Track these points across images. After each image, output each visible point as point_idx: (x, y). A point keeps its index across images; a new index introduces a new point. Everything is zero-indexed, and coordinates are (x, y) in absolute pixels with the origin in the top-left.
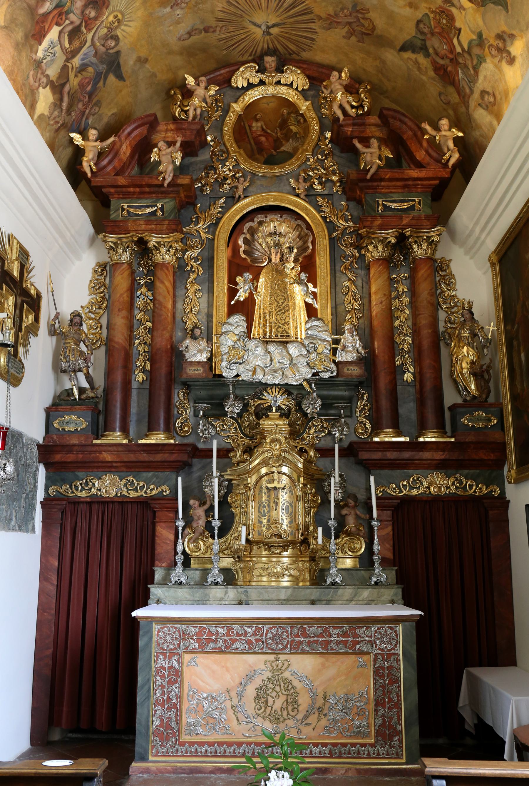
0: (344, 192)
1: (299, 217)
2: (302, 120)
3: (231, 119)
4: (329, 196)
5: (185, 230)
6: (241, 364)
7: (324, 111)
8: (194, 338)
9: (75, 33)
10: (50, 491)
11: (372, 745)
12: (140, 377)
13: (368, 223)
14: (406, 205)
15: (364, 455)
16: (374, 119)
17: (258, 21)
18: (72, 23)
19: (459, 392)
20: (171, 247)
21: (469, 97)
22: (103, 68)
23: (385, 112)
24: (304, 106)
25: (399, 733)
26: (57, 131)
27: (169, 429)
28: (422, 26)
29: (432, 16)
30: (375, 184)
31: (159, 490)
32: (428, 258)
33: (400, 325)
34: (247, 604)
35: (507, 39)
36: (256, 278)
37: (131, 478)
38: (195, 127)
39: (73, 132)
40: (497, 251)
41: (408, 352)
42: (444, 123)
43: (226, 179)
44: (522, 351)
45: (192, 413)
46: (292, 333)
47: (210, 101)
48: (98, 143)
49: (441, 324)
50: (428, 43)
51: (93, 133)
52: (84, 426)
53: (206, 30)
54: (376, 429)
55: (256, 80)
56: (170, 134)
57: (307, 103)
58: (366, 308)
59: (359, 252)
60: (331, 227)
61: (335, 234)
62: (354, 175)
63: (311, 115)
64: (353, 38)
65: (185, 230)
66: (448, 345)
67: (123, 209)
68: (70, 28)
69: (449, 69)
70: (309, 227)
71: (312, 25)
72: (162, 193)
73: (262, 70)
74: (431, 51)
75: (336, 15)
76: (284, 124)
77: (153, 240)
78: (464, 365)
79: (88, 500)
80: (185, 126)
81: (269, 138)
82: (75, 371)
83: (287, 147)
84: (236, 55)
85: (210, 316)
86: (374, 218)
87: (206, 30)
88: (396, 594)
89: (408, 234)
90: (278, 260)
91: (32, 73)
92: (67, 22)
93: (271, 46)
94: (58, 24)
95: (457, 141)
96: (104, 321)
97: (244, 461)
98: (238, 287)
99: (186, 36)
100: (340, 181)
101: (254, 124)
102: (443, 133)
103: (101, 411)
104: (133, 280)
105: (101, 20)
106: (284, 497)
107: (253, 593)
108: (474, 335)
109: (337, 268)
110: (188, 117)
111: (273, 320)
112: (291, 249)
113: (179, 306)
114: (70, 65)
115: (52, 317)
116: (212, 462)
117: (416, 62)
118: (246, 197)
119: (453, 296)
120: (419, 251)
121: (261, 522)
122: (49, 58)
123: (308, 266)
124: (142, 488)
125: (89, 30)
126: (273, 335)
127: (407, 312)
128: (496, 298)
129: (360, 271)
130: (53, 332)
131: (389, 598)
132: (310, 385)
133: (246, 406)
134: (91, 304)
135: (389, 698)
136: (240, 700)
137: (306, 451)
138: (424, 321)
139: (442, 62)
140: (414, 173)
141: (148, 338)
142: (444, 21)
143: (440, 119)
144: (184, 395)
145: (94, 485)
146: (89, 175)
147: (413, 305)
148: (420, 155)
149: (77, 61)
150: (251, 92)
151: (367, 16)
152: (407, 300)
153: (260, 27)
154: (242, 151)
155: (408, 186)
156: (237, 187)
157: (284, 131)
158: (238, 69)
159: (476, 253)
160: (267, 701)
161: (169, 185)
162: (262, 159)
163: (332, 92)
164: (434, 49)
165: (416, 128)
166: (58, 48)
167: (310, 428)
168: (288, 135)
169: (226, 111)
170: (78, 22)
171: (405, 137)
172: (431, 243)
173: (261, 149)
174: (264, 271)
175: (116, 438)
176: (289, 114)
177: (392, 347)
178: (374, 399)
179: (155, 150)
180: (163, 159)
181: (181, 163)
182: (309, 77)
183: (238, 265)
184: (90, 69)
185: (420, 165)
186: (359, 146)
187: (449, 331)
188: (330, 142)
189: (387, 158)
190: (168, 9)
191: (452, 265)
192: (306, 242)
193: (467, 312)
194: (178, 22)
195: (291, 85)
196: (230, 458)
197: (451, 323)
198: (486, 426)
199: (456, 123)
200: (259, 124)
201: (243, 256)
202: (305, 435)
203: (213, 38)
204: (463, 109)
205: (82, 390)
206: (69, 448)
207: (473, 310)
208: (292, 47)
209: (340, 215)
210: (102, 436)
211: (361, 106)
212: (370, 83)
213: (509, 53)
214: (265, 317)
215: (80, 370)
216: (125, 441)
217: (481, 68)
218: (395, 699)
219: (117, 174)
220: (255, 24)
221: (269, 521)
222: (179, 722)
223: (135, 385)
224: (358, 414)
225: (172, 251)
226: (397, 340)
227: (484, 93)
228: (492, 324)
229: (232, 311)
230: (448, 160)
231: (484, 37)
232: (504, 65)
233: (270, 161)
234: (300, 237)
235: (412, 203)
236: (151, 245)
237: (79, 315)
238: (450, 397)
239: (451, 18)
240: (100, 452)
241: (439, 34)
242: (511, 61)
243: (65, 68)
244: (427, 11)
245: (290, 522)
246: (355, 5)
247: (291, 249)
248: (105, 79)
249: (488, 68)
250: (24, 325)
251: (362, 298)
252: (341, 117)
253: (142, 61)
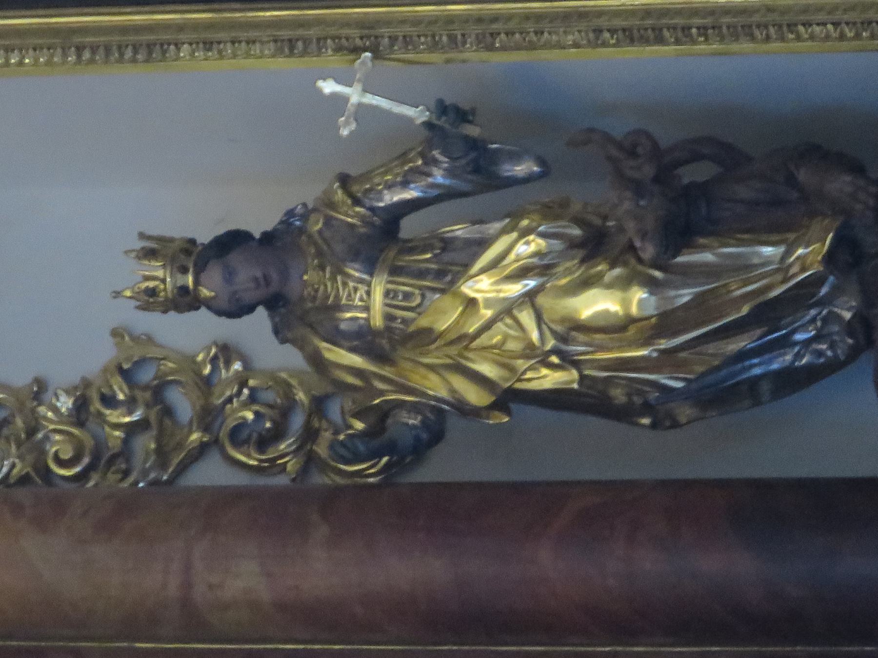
19: (791, 381)
66: (438, 420)
78: (597, 304)
108: (382, 240)
119: (81, 406)
128: (152, 48)
193: (214, 274)
197: (277, 434)
207: (205, 237)
228: (328, 87)
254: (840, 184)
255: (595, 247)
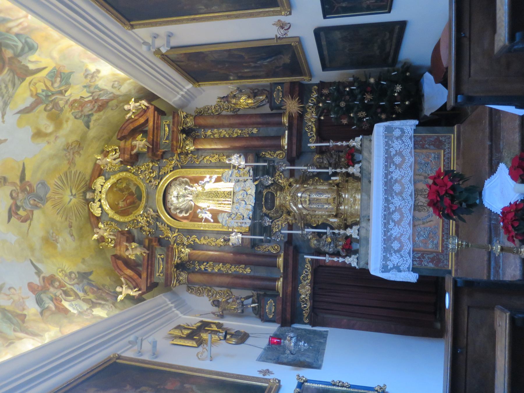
0: (158, 160)
1: (169, 185)
2: (120, 181)
3: (117, 217)
4: (160, 168)
5: (172, 243)
6: (243, 217)
7: (116, 170)
8: (229, 240)
9: (66, 293)
10: (306, 321)
11: (444, 152)
12: (248, 270)
13: (175, 148)
14: (167, 129)
15: (294, 154)
16: (122, 143)
17: (68, 200)
18: (61, 294)
19: (263, 105)
20: (181, 251)
21: (114, 94)
22: (85, 281)
23: (119, 137)
24: (113, 180)
25: (438, 137)
26: (116, 307)
27: (276, 256)
28: (77, 116)
29: (73, 111)
30: (155, 144)
31: (308, 262)
32: (194, 118)
33: (228, 134)
34: (369, 217)
35: (87, 73)
36: (199, 207)
37: (301, 278)
38: (119, 235)
39: (117, 299)
40: (193, 83)
41: (242, 130)
42: (126, 107)
43: (148, 222)
44: (243, 71)
45: (269, 244)
46: (229, 190)
47: (106, 228)
48: (124, 286)
49: (229, 113)
50: (87, 114)
51: (118, 289)
52: (272, 301)
53: (71, 227)
54: (280, 148)
55: (99, 203)
56: (122, 249)
57: (112, 177)
58: (218, 151)
59: (190, 154)
60: (175, 168)
61: (179, 166)
62: (150, 154)
63: (117, 176)
64: (81, 152)
65: (172, 243)
66: (239, 109)
67: (159, 275)
68: (63, 296)
69: (100, 104)
70: (175, 179)
71: (73, 172)
72: (152, 255)
73: (93, 200)
74: (90, 113)
75: (69, 160)
76: (121, 190)
77: (176, 260)
78: (250, 101)
79: (312, 301)
80: (118, 240)
81: (129, 198)
82: (243, 305)
83: (133, 189)
84: (85, 213)
85: (218, 233)
86: (172, 145)
87: (71, 227)
88: (367, 139)
89: (181, 127)
90: (191, 196)
91: (85, 317)
92: (60, 296)
93: (81, 195)
94: (61, 301)
95: (136, 101)
96: (218, 289)
97: (294, 216)
98: (204, 217)
99: (73, 237)
100: (152, 162)
101: (120, 205)
102: (131, 108)
103: (264, 291)
104: (197, 272)
105: (61, 279)
106: (314, 196)
107: (364, 213)
108: (234, 97)
109: (197, 165)
110: (114, 239)
111: (222, 199)
112: (185, 189)
113: (212, 248)
114: (82, 298)
115: (213, 316)
116: (294, 234)
117: (96, 120)
118: (157, 212)
120: (190, 123)
121: (327, 208)
122: (78, 308)
123: (195, 180)
124: (306, 272)
125: (65, 286)
126: (230, 200)
127: (221, 130)
128: (217, 84)
129: (200, 154)
130: (222, 316)
131: (368, 142)
132: (256, 180)
133: (267, 215)
134: (208, 295)
135: (420, 142)
136: (420, 220)
137: (290, 183)
138: (226, 122)
139: (96, 107)
140: (151, 124)
141: (228, 266)
142: (76, 105)
143: (125, 109)
144: (259, 248)
145: (304, 298)
146: (140, 292)
147: (218, 127)
148: (142, 120)
149: (81, 294)
150: (104, 207)
151: (70, 144)
152: (215, 131)
153: (71, 199)
154: (134, 212)
155: (157, 128)
156: (152, 216)
157: (125, 190)
158: (92, 213)
159: (193, 94)
160: (421, 206)
161: (148, 250)
162: (139, 202)
163: (107, 164)
164: (89, 111)
165: (129, 122)
166: (73, 303)
167: (279, 182)
168: (127, 188)
169: (112, 220)
170: (61, 291)
171: (132, 128)
172: (186, 116)
173: (133, 203)
174: (196, 204)
175: (279, 284)
176: (116, 187)
177: (238, 138)
178: (266, 148)
179: (129, 257)
180: (135, 253)
181: (137, 243)
182: (99, 176)
183: (193, 217)
184: (85, 288)
185: (147, 121)
186: (135, 151)
187: (232, 109)
188: (132, 167)
189: (142, 137)
190: (59, 245)
191: (199, 107)
192: (183, 182)
194: (65, 241)
195: (102, 186)
196: (293, 224)
198: (282, 91)
199: (128, 103)
200: (121, 203)
201: (188, 214)
202: (283, 185)
203: (75, 224)
204: (121, 98)
205: (253, 302)
206: (284, 310)
208: (83, 183)
209: (170, 163)
210: (278, 292)
211: (115, 150)
212: (104, 146)
213: (94, 72)
214: (220, 204)
215: (242, 302)
216: (281, 279)
217: (101, 87)
218: (420, 138)
219: (140, 277)
220: (70, 202)
221: (326, 204)
222: (432, 253)
223: (252, 274)
224: (272, 157)
225: (183, 250)
226: (236, 135)
227: (113, 87)
229: (216, 221)
230: (145, 106)
231: (85, 85)
232: (100, 75)
233: (140, 198)
234: (180, 184)
235: (166, 126)
236: (179, 261)
237: (213, 302)
238: (266, 109)
239: (75, 101)
240: (287, 293)
241: (82, 107)
242: (98, 71)
243: (84, 300)
244: (71, 113)
245: (327, 192)
246: (64, 150)
247: (185, 189)
248: (90, 280)
249: (101, 84)
250: (216, 329)
251: (213, 153)
252: (120, 159)
253: (84, 261)
254: (266, 92)
255: (249, 97)
